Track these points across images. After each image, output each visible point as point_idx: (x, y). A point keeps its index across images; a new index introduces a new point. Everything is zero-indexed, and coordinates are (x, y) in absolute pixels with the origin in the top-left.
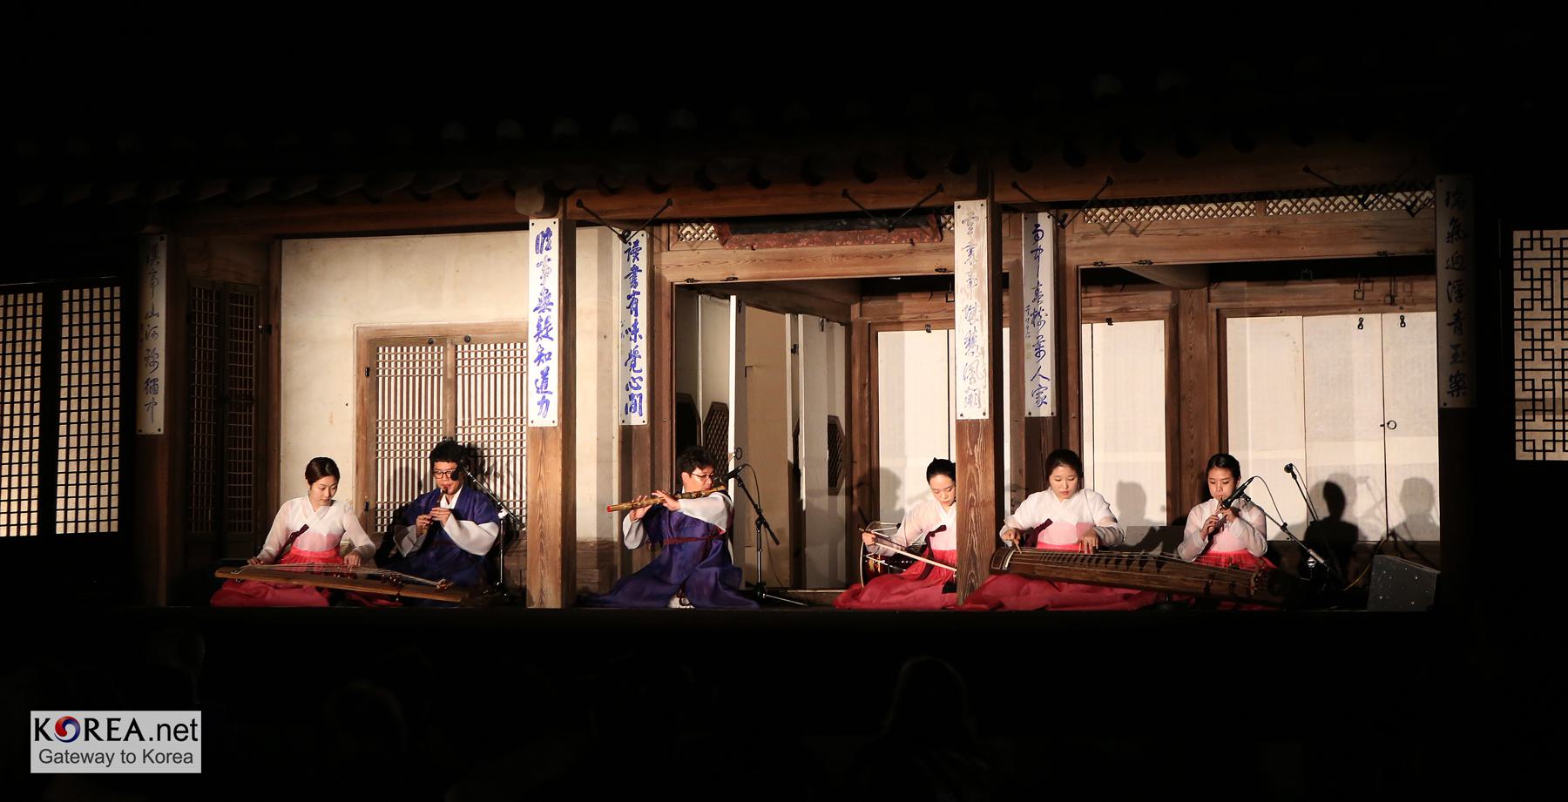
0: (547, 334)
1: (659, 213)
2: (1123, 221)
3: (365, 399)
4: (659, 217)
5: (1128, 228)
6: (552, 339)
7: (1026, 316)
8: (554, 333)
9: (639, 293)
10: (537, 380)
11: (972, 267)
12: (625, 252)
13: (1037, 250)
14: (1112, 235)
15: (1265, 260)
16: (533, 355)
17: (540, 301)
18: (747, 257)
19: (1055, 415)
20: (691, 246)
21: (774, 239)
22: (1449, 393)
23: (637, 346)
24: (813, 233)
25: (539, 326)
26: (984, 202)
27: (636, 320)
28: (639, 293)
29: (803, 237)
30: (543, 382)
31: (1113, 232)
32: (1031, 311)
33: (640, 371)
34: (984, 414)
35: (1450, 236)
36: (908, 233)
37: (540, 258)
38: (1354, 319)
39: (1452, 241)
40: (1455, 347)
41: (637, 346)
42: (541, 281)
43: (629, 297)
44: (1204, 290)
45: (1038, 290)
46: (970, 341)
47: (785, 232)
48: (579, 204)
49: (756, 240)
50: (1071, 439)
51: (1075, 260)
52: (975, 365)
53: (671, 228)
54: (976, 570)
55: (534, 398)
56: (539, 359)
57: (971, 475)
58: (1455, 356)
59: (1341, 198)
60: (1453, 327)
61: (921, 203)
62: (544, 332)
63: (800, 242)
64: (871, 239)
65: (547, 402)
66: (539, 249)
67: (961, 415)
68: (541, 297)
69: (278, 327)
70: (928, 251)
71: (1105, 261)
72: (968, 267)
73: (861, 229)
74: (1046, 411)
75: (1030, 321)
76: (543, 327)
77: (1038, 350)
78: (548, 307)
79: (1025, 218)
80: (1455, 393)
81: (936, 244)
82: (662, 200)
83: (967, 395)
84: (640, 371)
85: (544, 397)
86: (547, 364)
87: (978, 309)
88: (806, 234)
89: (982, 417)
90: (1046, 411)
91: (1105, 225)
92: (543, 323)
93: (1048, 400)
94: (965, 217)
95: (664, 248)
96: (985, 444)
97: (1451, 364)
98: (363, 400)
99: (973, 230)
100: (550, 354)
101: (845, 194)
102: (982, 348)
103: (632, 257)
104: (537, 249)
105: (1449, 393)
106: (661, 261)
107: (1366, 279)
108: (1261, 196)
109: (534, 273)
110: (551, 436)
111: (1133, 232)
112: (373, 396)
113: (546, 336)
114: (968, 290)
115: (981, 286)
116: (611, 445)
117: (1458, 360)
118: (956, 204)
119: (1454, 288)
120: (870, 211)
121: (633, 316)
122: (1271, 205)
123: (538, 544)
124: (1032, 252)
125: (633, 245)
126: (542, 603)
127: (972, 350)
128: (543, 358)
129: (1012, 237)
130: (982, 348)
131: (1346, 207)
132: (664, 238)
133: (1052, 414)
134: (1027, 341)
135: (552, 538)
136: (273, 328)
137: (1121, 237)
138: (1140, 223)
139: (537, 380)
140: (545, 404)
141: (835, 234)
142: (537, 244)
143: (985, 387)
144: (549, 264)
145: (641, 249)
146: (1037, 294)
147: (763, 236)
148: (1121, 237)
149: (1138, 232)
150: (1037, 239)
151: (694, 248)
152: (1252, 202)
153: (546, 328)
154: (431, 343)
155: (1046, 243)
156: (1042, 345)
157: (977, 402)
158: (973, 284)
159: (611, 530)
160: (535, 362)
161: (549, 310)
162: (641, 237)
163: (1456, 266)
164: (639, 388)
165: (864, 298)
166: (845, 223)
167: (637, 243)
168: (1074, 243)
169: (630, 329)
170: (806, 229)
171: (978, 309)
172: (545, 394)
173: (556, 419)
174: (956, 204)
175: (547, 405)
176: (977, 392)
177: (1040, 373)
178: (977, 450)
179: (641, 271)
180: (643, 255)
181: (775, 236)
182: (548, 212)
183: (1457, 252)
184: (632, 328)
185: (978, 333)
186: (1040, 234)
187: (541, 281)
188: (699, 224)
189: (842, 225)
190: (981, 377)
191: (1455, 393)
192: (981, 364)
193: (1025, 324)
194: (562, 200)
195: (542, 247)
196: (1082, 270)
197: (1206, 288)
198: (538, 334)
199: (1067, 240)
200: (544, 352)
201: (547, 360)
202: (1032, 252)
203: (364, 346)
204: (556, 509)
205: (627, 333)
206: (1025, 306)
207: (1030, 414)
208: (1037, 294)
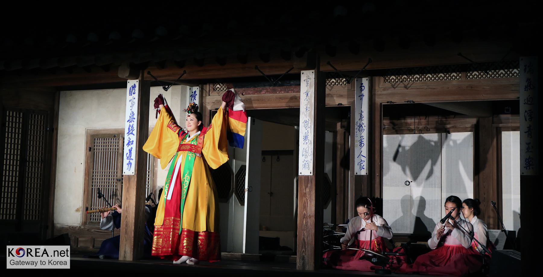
0: (132, 132)
1: (181, 77)
2: (401, 82)
3: (89, 161)
4: (181, 79)
6: (134, 135)
7: (356, 127)
8: (135, 132)
10: (127, 154)
11: (307, 102)
12: (190, 96)
13: (361, 96)
14: (396, 89)
15: (466, 101)
16: (126, 142)
17: (130, 117)
19: (368, 174)
20: (218, 93)
21: (252, 91)
22: (524, 167)
24: (268, 87)
25: (129, 129)
26: (314, 71)
29: (264, 89)
30: (129, 154)
31: (396, 87)
32: (358, 125)
34: (311, 173)
35: (526, 87)
37: (131, 97)
39: (527, 91)
40: (528, 144)
42: (131, 108)
44: (491, 118)
45: (361, 114)
46: (306, 138)
47: (256, 87)
48: (149, 73)
49: (244, 91)
50: (376, 186)
51: (379, 100)
52: (307, 149)
53: (211, 85)
55: (126, 161)
56: (128, 144)
57: (305, 203)
58: (528, 149)
59: (502, 71)
60: (527, 133)
61: (289, 71)
62: (131, 131)
63: (262, 92)
64: (292, 90)
65: (131, 164)
66: (131, 94)
67: (301, 173)
69: (57, 129)
71: (393, 101)
72: (306, 102)
73: (288, 86)
74: (364, 172)
75: (358, 129)
76: (131, 129)
77: (361, 143)
78: (133, 120)
79: (357, 81)
80: (528, 168)
82: (181, 71)
83: (304, 163)
85: (130, 161)
86: (131, 146)
87: (310, 122)
88: (264, 88)
89: (309, 174)
90: (364, 172)
91: (393, 84)
92: (131, 127)
93: (365, 167)
94: (305, 78)
95: (207, 95)
96: (311, 187)
97: (526, 152)
98: (88, 162)
99: (309, 85)
100: (133, 141)
101: (256, 68)
102: (311, 141)
103: (193, 99)
104: (130, 93)
105: (524, 167)
106: (206, 101)
108: (464, 69)
109: (128, 104)
110: (132, 179)
111: (406, 87)
112: (92, 160)
113: (132, 133)
114: (306, 113)
117: (530, 150)
118: (302, 72)
119: (528, 114)
120: (268, 76)
122: (469, 74)
123: (125, 230)
124: (359, 96)
125: (194, 93)
126: (125, 257)
127: (306, 142)
128: (130, 143)
129: (352, 90)
130: (311, 141)
131: (504, 75)
132: (208, 90)
133: (366, 174)
134: (356, 139)
135: (130, 227)
136: (55, 129)
137: (400, 89)
138: (409, 83)
139: (127, 154)
140: (130, 164)
141: (276, 88)
142: (130, 91)
143: (311, 160)
144: (134, 100)
146: (361, 116)
147: (247, 89)
148: (400, 89)
150: (362, 90)
152: (460, 72)
153: (132, 130)
154: (115, 136)
155: (366, 92)
156: (363, 140)
157: (308, 167)
160: (127, 145)
161: (133, 121)
162: (196, 89)
163: (529, 103)
165: (343, 120)
166: (280, 83)
167: (195, 92)
168: (379, 93)
170: (265, 86)
171: (310, 122)
172: (130, 160)
173: (134, 172)
174: (302, 72)
175: (131, 165)
176: (308, 162)
177: (362, 154)
178: (308, 190)
180: (197, 97)
181: (252, 89)
182: (134, 76)
183: (529, 96)
185: (309, 134)
186: (363, 88)
187: (131, 108)
188: (222, 84)
189: (279, 83)
190: (309, 155)
191: (528, 168)
192: (310, 149)
193: (356, 130)
194: (141, 71)
195: (132, 92)
196: (384, 105)
197: (492, 117)
198: (128, 132)
199: (376, 91)
201: (132, 144)
202: (359, 96)
203: (89, 138)
204: (132, 213)
206: (356, 122)
207: (357, 173)
208: (361, 116)
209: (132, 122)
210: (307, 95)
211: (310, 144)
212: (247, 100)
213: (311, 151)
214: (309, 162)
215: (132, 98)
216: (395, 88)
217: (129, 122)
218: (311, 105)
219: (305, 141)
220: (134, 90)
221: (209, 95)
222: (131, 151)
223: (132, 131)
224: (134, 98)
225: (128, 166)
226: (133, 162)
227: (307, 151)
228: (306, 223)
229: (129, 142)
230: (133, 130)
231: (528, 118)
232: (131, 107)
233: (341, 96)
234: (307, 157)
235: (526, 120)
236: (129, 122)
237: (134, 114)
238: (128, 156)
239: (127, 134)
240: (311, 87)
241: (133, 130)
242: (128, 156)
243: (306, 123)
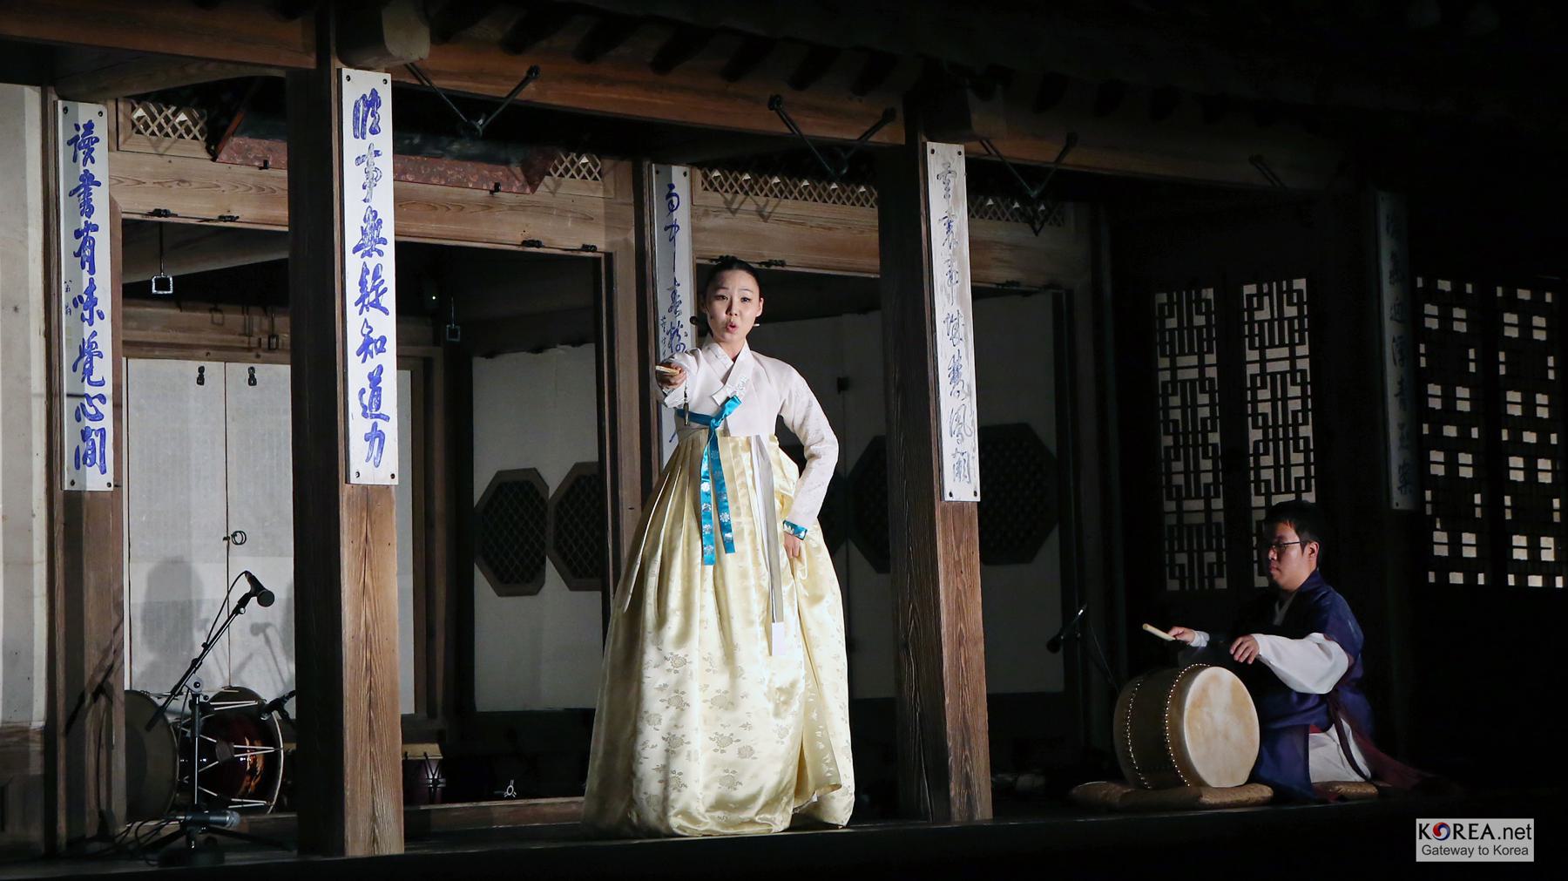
0: (377, 300)
5: (754, 208)
6: (385, 311)
7: (662, 335)
8: (389, 300)
9: (96, 228)
10: (363, 391)
11: (951, 251)
13: (672, 226)
14: (737, 215)
17: (364, 232)
18: (250, 182)
20: (155, 146)
23: (94, 334)
25: (362, 283)
27: (92, 280)
28: (96, 228)
30: (372, 396)
32: (668, 327)
33: (101, 384)
34: (975, 494)
36: (490, 171)
38: (192, 367)
41: (94, 334)
43: (78, 234)
45: (675, 292)
49: (270, 150)
54: (971, 753)
56: (364, 350)
62: (372, 296)
64: (442, 175)
65: (381, 436)
68: (365, 225)
70: (511, 208)
76: (369, 286)
78: (379, 247)
79: (657, 172)
81: (528, 197)
82: (521, 67)
84: (101, 384)
85: (375, 425)
86: (378, 359)
87: (961, 321)
92: (369, 278)
99: (950, 192)
100: (383, 340)
101: (774, 103)
102: (969, 387)
103: (81, 156)
104: (356, 127)
107: (213, 306)
113: (376, 304)
114: (949, 289)
115: (963, 286)
116: (30, 531)
121: (85, 273)
124: (666, 228)
125: (82, 131)
127: (957, 388)
128: (371, 347)
130: (969, 387)
139: (363, 391)
140: (377, 440)
142: (356, 118)
143: (974, 451)
145: (97, 140)
146: (674, 299)
149: (766, 214)
151: (161, 150)
153: (375, 288)
158: (954, 281)
159: (29, 704)
161: (380, 253)
164: (98, 417)
167: (89, 127)
169: (80, 298)
172: (378, 420)
175: (382, 442)
176: (965, 456)
179: (98, 184)
183: (1397, 299)
184: (85, 297)
186: (675, 199)
190: (969, 433)
192: (968, 412)
195: (364, 125)
198: (361, 300)
200: (375, 336)
205: (76, 305)
208: (674, 299)
209: (375, 253)
210: (949, 226)
211: (967, 395)
212: (274, 191)
213: (973, 421)
214: (968, 456)
215: (365, 152)
216: (734, 212)
217: (363, 256)
218: (961, 264)
219: (953, 384)
220: (373, 115)
221: (118, 149)
222: (379, 380)
223: (378, 295)
224: (377, 153)
225: (372, 446)
226: (391, 429)
227: (961, 421)
228: (966, 664)
229: (368, 341)
230: (380, 290)
231: (1398, 358)
232: (364, 188)
233: (587, 219)
234: (963, 439)
235: (1395, 363)
236: (363, 256)
237: (380, 222)
238: (366, 403)
239: (357, 304)
240: (956, 201)
241: (380, 290)
242: (366, 403)
243: (952, 324)
